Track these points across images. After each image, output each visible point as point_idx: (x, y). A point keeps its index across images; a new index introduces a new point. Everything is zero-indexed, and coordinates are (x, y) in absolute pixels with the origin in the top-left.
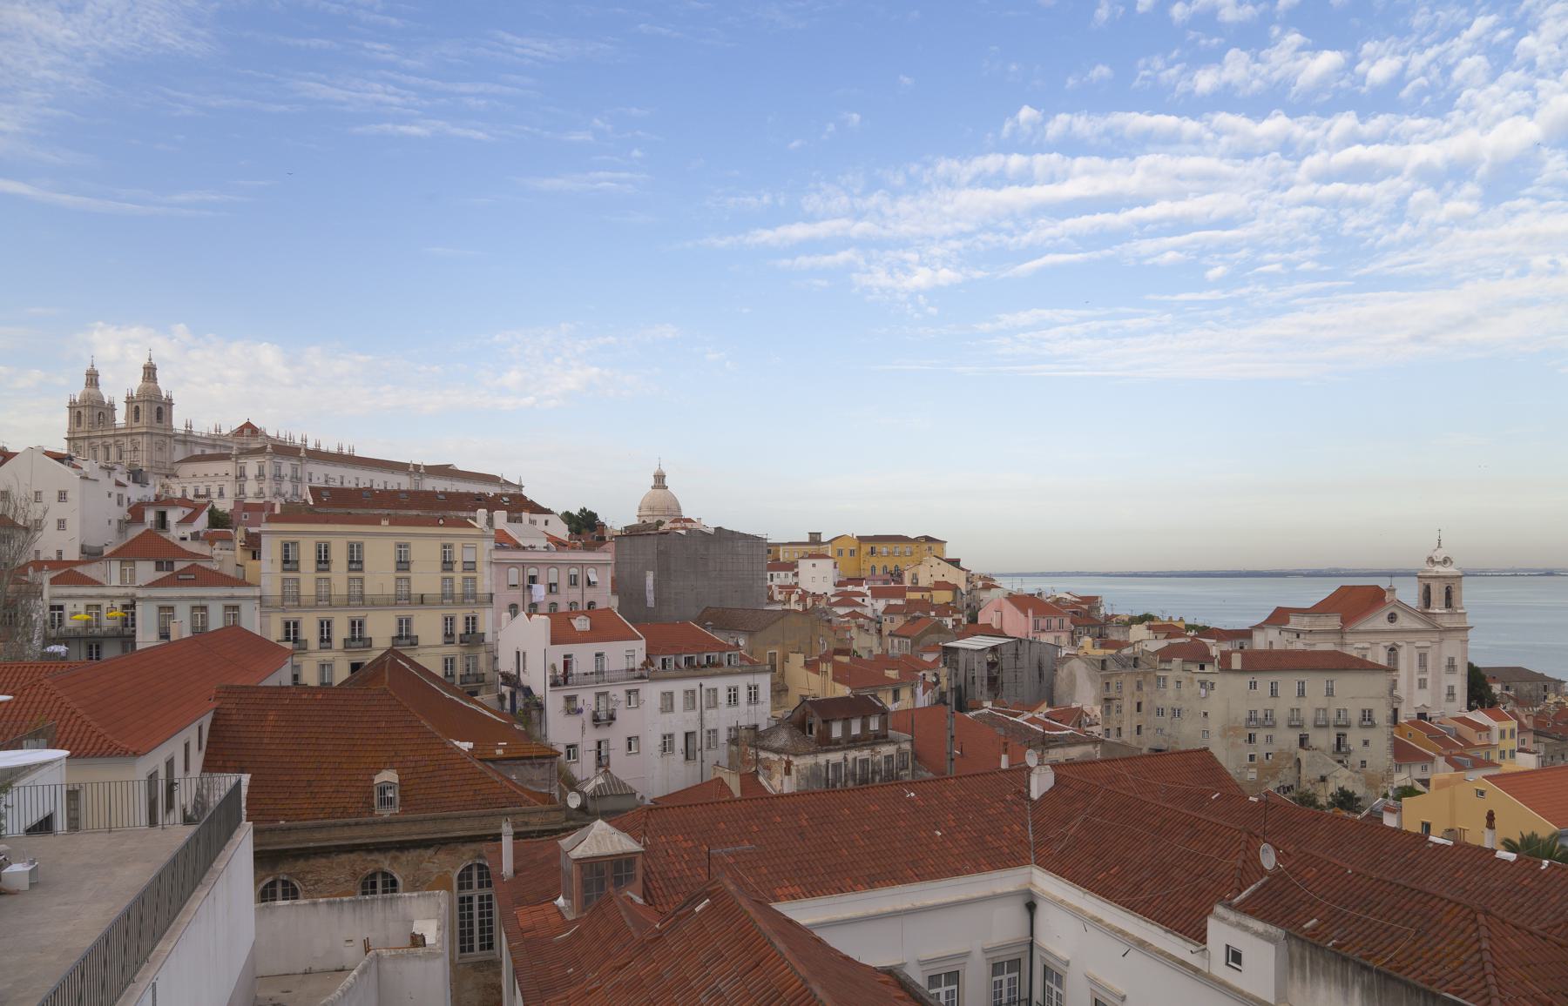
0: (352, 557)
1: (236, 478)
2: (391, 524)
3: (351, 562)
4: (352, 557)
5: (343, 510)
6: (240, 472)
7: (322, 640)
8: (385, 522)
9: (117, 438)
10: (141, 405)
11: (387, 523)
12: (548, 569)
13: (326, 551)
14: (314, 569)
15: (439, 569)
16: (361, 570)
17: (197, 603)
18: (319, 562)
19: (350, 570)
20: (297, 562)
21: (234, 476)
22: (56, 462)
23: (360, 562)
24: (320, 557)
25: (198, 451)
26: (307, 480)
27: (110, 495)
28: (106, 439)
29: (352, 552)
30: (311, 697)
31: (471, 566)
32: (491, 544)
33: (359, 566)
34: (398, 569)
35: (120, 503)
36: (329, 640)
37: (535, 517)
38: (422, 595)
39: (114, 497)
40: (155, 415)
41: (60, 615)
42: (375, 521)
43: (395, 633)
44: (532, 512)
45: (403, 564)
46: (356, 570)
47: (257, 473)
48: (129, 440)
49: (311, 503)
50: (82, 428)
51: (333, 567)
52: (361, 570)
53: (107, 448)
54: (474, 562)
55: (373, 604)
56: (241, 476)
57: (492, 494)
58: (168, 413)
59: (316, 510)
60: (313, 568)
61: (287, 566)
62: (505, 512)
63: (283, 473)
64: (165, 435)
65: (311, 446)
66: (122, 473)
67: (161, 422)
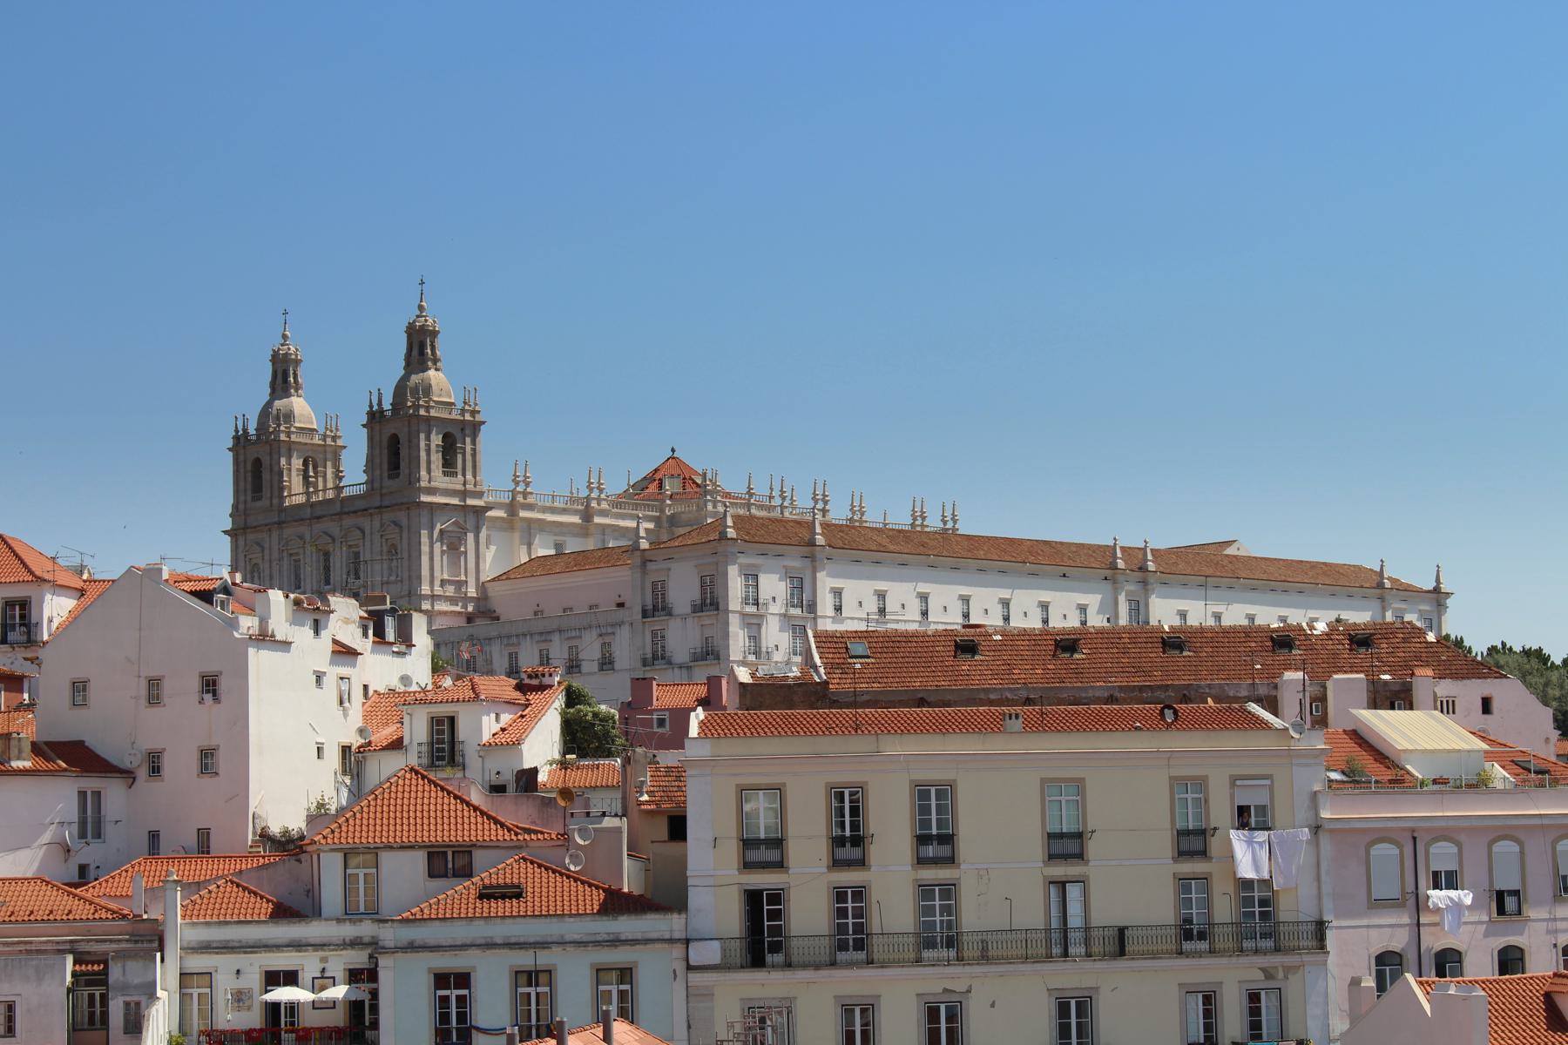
0: (925, 824)
1: (645, 614)
2: (1032, 727)
3: (922, 840)
4: (925, 824)
9: (348, 522)
12: (1490, 845)
13: (855, 811)
15: (1165, 844)
16: (951, 860)
17: (525, 960)
18: (838, 842)
19: (921, 861)
20: (778, 843)
23: (947, 839)
26: (830, 612)
28: (318, 527)
29: (924, 810)
33: (944, 851)
38: (1121, 931)
46: (936, 861)
47: (695, 594)
48: (377, 524)
50: (265, 502)
51: (875, 852)
52: (951, 860)
55: (985, 958)
56: (655, 608)
57: (1321, 627)
60: (821, 848)
61: (754, 855)
63: (764, 595)
65: (839, 513)
66: (347, 621)
67: (455, 474)
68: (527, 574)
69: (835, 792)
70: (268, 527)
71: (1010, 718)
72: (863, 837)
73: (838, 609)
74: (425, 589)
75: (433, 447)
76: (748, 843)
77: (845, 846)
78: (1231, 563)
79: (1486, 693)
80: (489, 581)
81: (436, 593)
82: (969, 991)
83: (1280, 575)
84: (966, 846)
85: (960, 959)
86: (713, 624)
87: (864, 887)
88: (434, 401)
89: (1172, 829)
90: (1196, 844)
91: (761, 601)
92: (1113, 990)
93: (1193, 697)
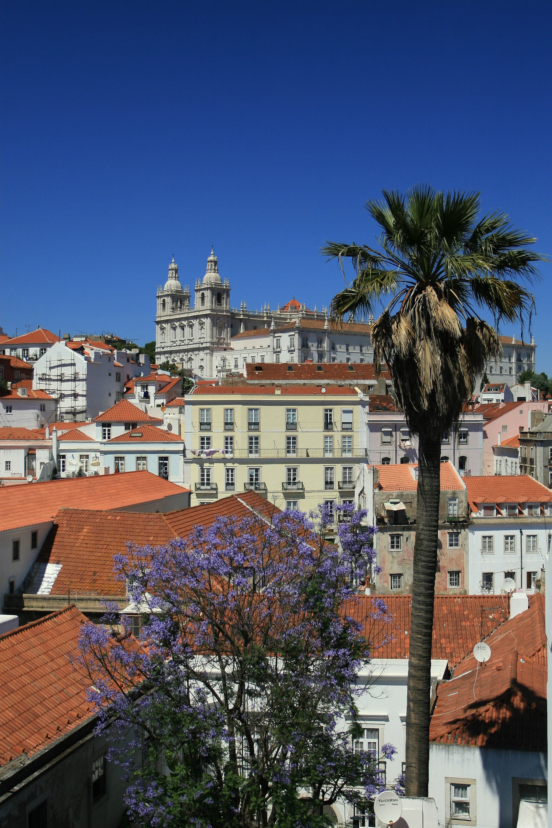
3: (250, 424)
5: (268, 382)
6: (277, 343)
7: (227, 484)
10: (205, 292)
16: (258, 430)
17: (139, 455)
18: (226, 424)
19: (250, 430)
20: (209, 424)
21: (271, 347)
22: (72, 351)
23: (257, 424)
27: (110, 374)
30: (113, 518)
33: (256, 427)
35: (118, 379)
36: (233, 484)
39: (114, 377)
41: (64, 462)
43: (285, 480)
45: (291, 426)
47: (289, 344)
49: (245, 376)
52: (258, 430)
53: (183, 328)
54: (351, 423)
59: (248, 382)
61: (203, 427)
76: (201, 424)
84: (262, 426)
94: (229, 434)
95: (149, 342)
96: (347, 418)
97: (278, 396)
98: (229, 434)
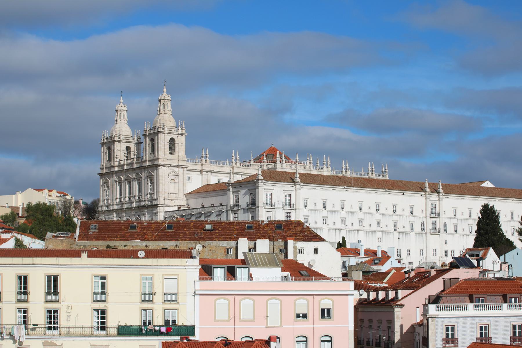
0: (49, 288)
2: (89, 256)
3: (48, 293)
8: (84, 255)
11: (84, 255)
13: (25, 283)
14: (15, 299)
15: (138, 298)
16: (58, 301)
18: (20, 293)
23: (56, 293)
24: (21, 289)
25: (214, 180)
26: (302, 206)
31: (173, 297)
32: (196, 273)
33: (56, 298)
34: (94, 301)
37: (301, 244)
40: (168, 146)
42: (76, 254)
44: (296, 240)
51: (31, 297)
54: (177, 294)
55: (69, 334)
58: (180, 144)
62: (267, 241)
64: (178, 166)
68: (200, 191)
69: (19, 277)
70: (111, 173)
71: (83, 253)
72: (27, 292)
73: (306, 206)
74: (161, 196)
75: (166, 143)
77: (51, 295)
78: (479, 189)
79: (316, 247)
80: (189, 193)
81: (165, 198)
82: (62, 345)
83: (499, 194)
85: (60, 335)
86: (254, 212)
87: (27, 309)
88: (166, 126)
89: (140, 292)
90: (148, 297)
91: (273, 203)
92: (114, 347)
93: (206, 246)
94: (23, 305)
95: (96, 198)
96: (171, 286)
97: (84, 258)
98: (23, 305)
